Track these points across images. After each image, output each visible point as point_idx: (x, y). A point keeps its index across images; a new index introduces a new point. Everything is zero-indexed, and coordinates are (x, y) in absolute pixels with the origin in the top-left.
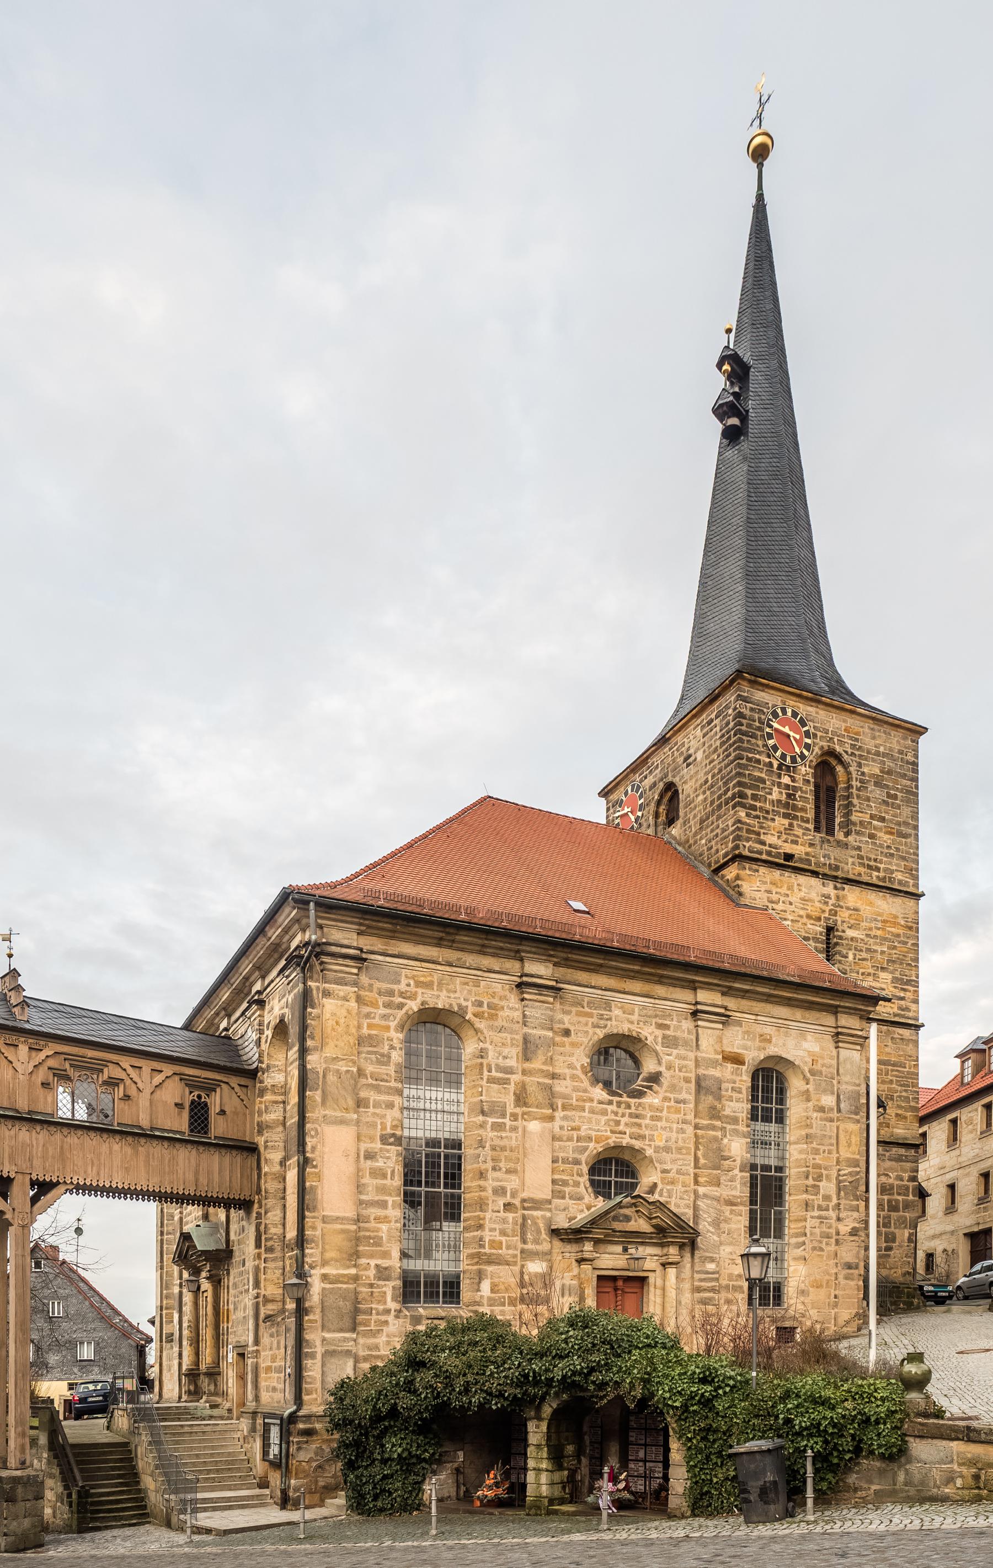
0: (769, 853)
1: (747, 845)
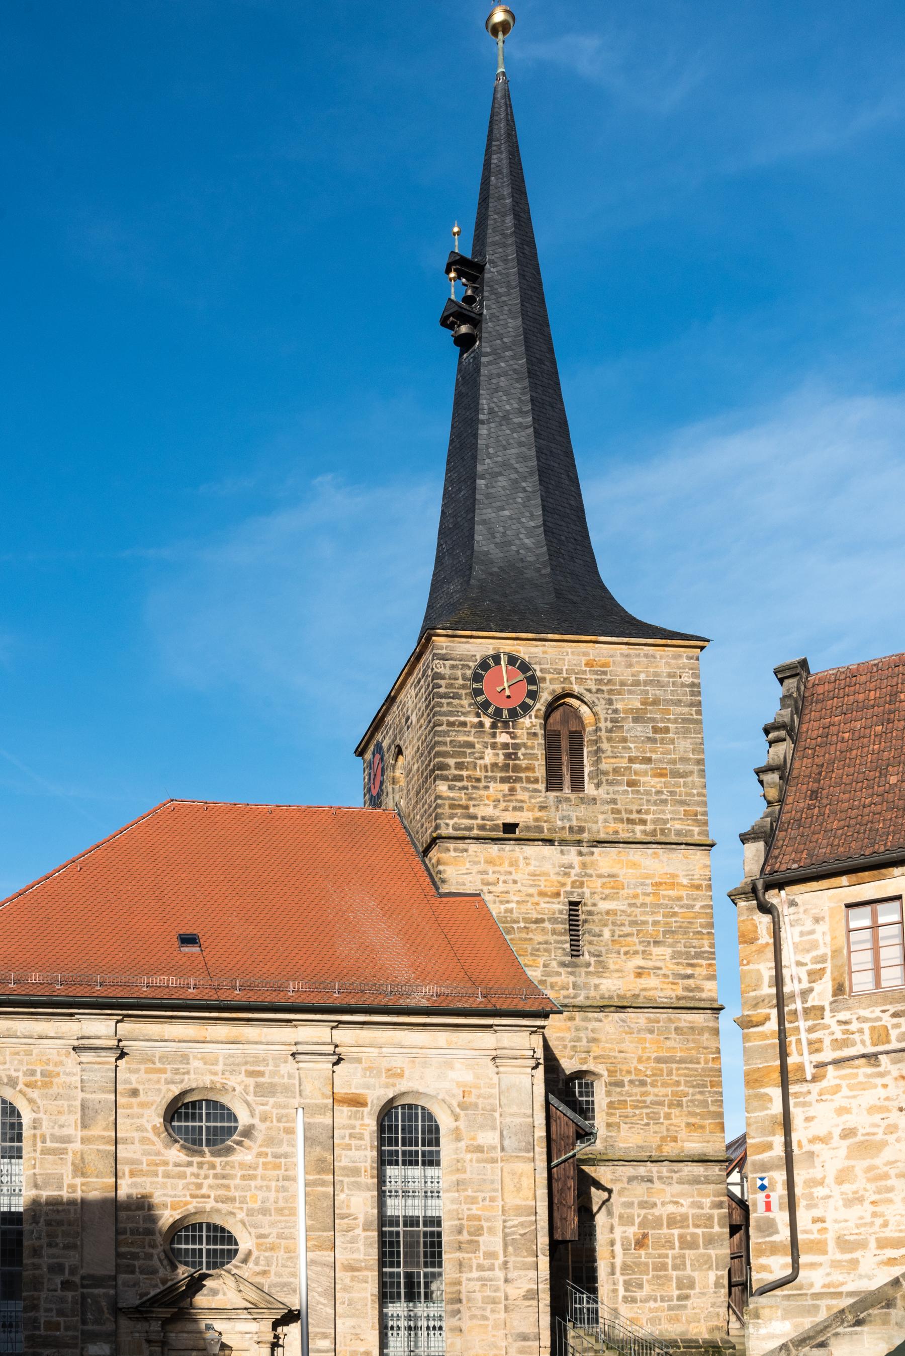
0: (482, 828)
1: (451, 822)
